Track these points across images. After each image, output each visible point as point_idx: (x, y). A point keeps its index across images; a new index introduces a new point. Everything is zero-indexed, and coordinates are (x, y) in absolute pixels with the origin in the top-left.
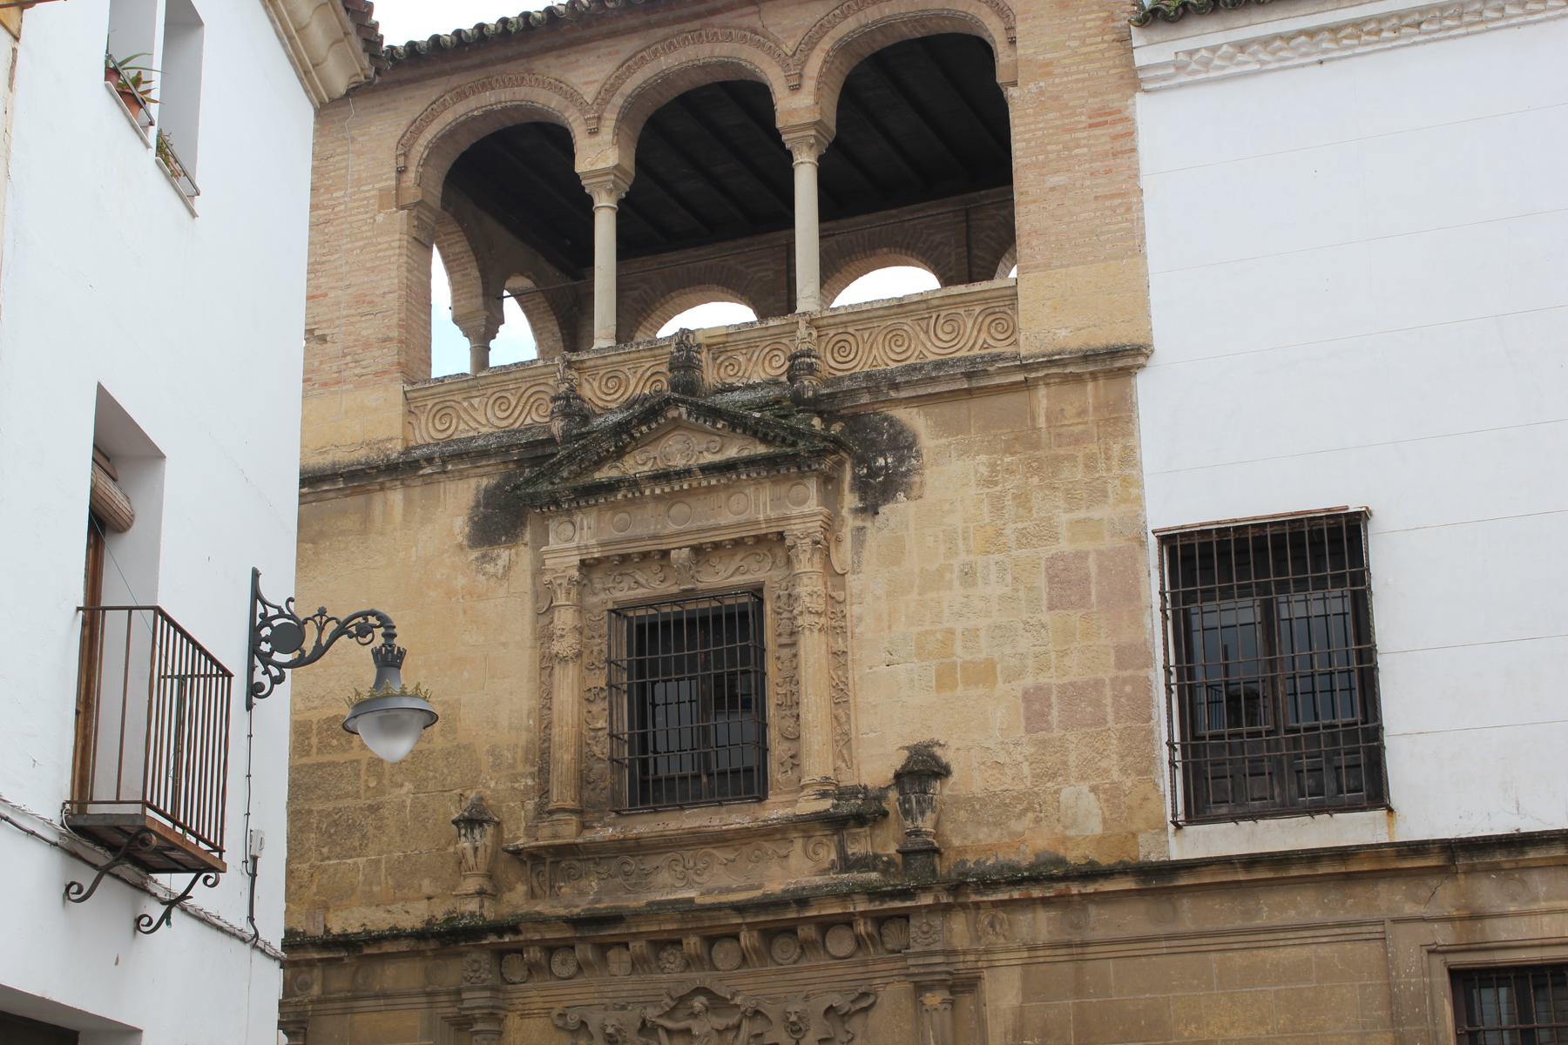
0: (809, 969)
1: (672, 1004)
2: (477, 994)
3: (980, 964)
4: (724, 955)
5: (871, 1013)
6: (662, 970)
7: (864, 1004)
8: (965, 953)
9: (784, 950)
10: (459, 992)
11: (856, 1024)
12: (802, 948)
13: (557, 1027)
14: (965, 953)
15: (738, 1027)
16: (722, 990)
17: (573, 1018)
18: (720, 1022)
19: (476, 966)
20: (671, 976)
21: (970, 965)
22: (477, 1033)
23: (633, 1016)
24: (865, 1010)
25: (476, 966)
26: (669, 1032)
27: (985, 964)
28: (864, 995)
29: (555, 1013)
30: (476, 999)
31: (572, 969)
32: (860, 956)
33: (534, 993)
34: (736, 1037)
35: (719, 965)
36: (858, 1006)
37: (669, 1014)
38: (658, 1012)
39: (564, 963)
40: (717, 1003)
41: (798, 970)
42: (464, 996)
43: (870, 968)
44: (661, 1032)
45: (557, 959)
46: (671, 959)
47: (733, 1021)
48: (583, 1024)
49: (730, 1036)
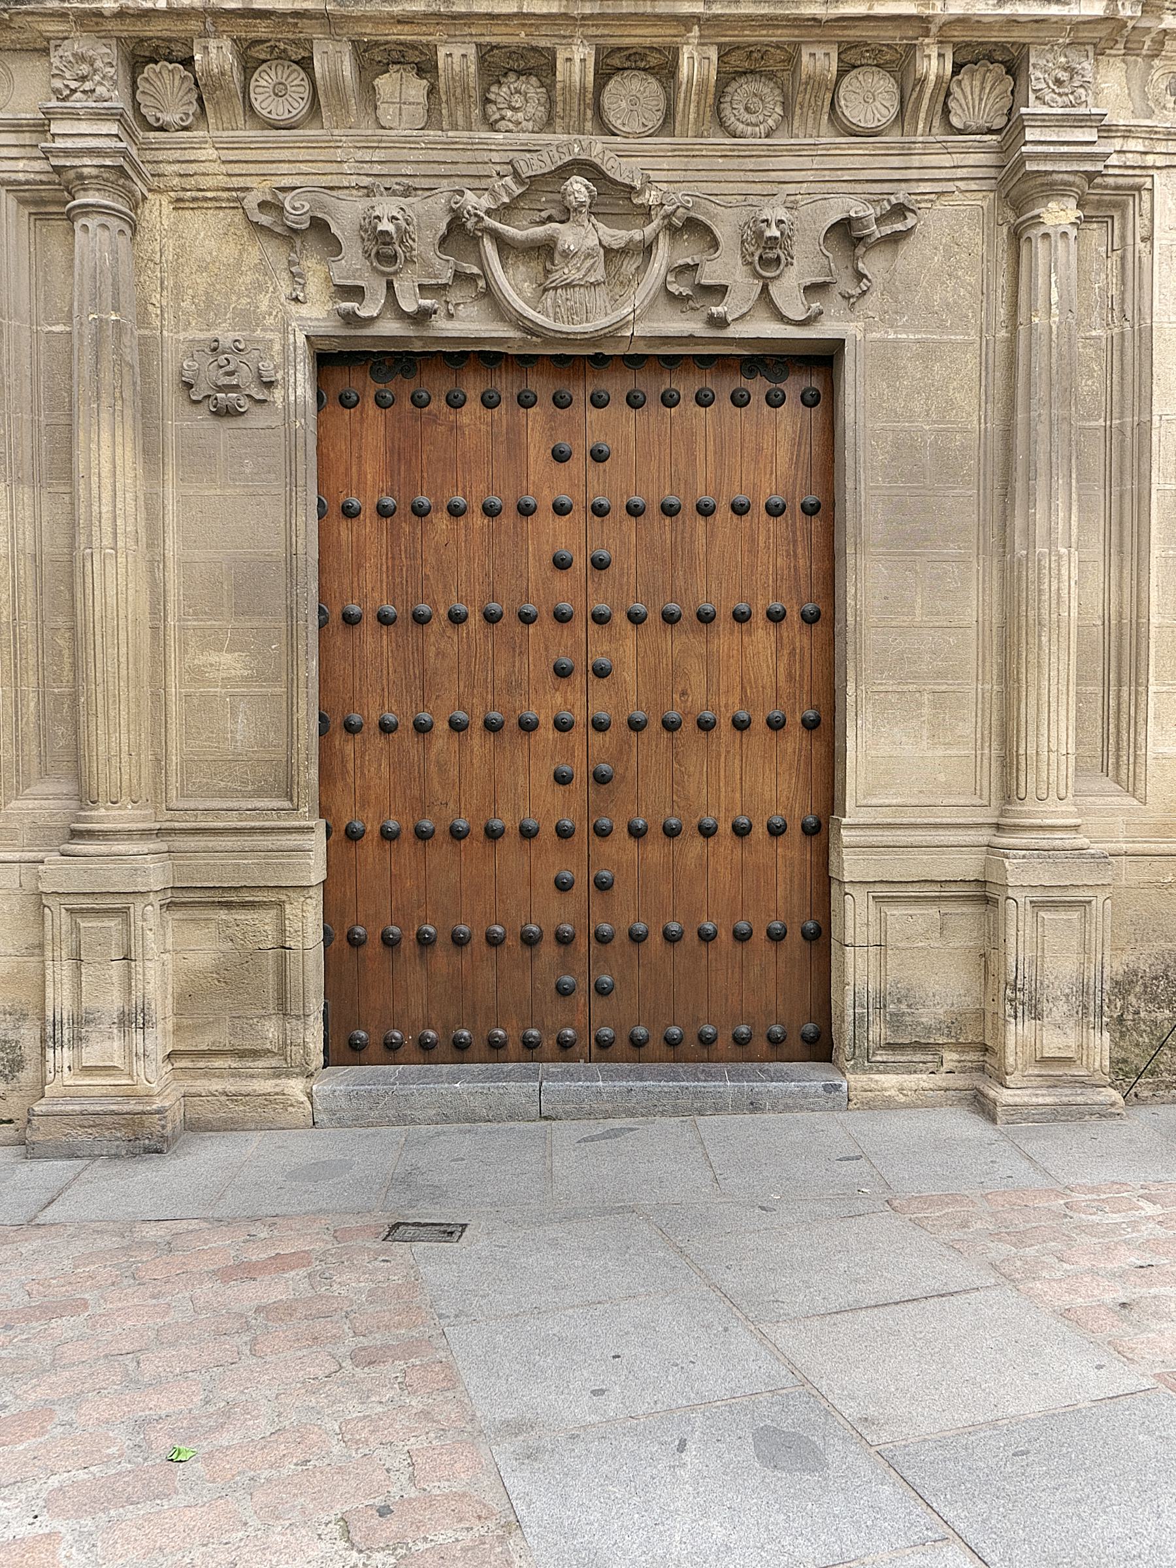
0: (795, 151)
1: (518, 191)
2: (84, 127)
3: (1150, 160)
4: (630, 99)
5: (905, 248)
6: (492, 127)
7: (899, 227)
8: (1128, 133)
9: (755, 102)
10: (41, 127)
11: (873, 264)
12: (787, 106)
13: (258, 227)
14: (1128, 133)
15: (648, 249)
16: (622, 170)
17: (298, 208)
18: (616, 236)
19: (85, 69)
20: (522, 136)
21: (1131, 159)
22: (87, 209)
23: (429, 214)
24: (896, 239)
25: (85, 69)
26: (504, 245)
27: (1161, 161)
28: (900, 211)
29: (251, 201)
30: (87, 135)
31: (295, 104)
32: (894, 137)
33: (208, 152)
34: (642, 269)
35: (614, 119)
36: (887, 230)
37: (504, 211)
38: (486, 202)
39: (279, 91)
40: (614, 197)
41: (774, 152)
42: (55, 128)
43: (916, 161)
44: (489, 248)
45: (264, 80)
46: (521, 98)
47: (649, 230)
48: (319, 226)
49: (629, 266)
